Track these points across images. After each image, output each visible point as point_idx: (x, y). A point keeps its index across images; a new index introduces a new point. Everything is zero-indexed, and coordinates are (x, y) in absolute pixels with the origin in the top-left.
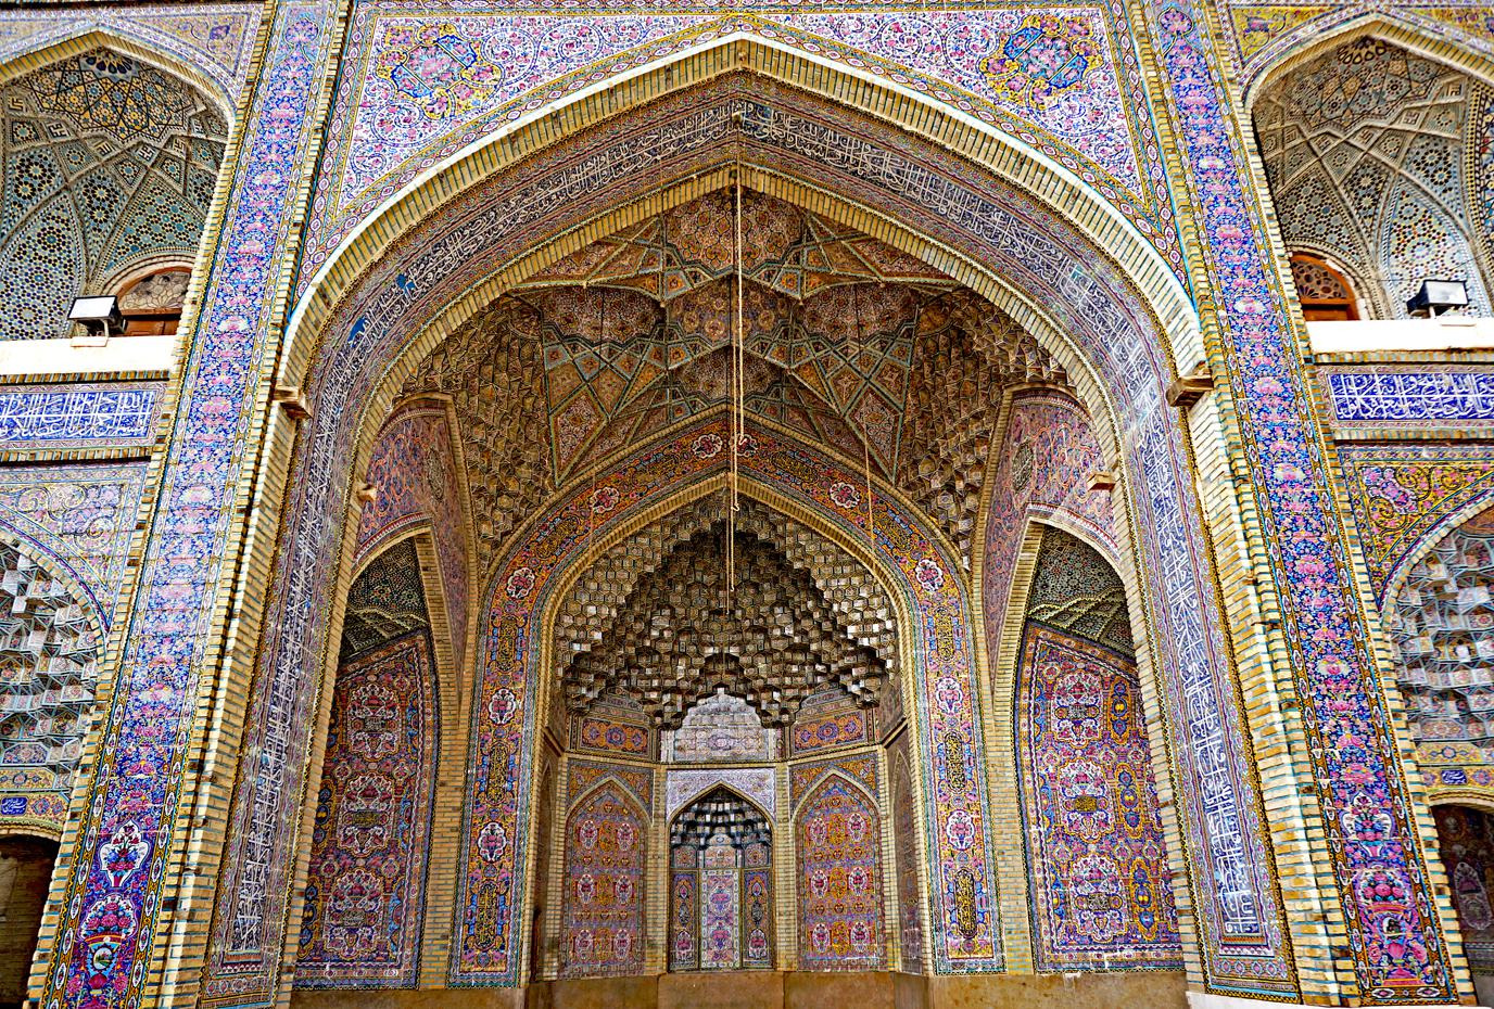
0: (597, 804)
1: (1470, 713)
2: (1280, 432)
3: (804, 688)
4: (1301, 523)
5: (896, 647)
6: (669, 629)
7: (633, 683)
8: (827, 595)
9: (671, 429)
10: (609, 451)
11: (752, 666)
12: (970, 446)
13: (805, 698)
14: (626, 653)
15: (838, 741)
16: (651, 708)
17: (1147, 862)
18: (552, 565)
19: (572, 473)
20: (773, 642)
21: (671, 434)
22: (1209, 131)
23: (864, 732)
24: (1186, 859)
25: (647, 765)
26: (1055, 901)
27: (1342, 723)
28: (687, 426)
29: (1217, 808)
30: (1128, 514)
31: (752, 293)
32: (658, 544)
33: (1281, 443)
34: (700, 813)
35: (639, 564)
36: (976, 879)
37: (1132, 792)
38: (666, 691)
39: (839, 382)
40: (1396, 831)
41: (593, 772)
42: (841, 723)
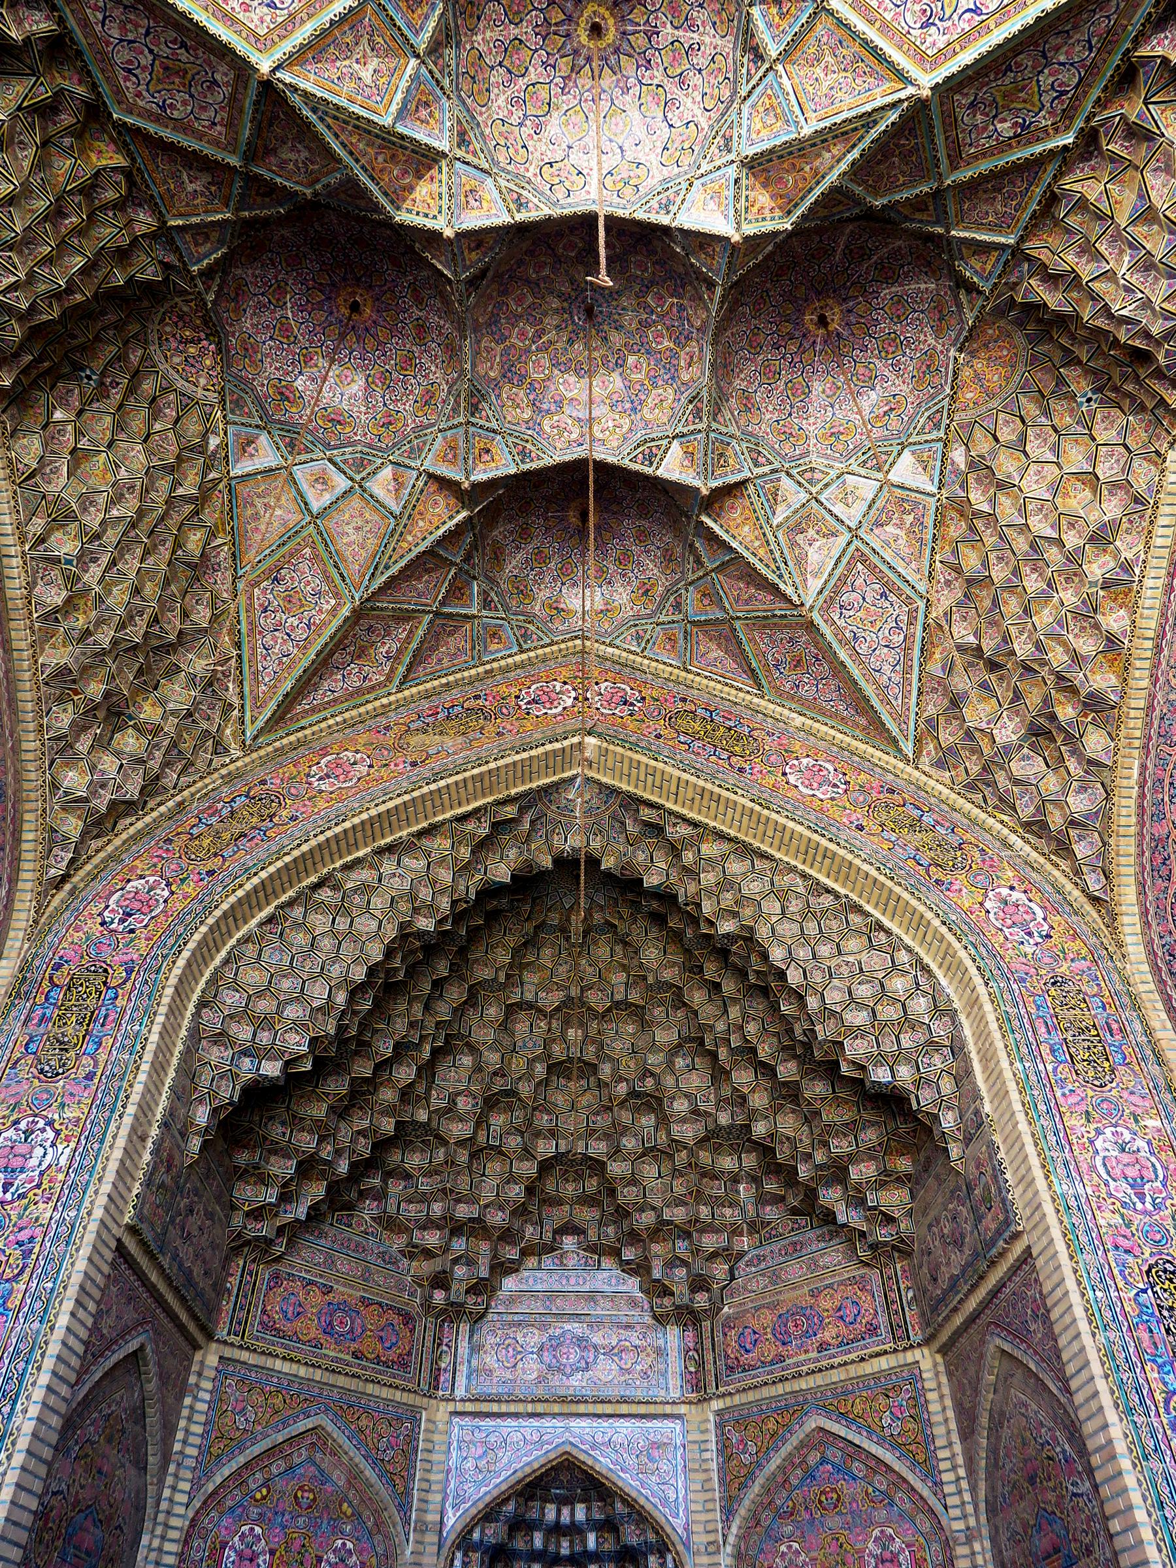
0: (279, 1484)
3: (736, 1231)
5: (963, 1076)
6: (468, 1093)
7: (392, 1209)
8: (794, 977)
9: (481, 669)
10: (359, 692)
11: (633, 1181)
12: (1087, 614)
13: (741, 1255)
14: (373, 1130)
15: (822, 1347)
16: (426, 1267)
18: (211, 873)
19: (279, 718)
20: (675, 1128)
21: (479, 678)
23: (882, 1319)
25: (406, 1398)
28: (507, 670)
31: (631, 360)
32: (445, 876)
34: (519, 1525)
35: (404, 906)
38: (457, 1229)
39: (800, 538)
41: (278, 1401)
42: (826, 1303)
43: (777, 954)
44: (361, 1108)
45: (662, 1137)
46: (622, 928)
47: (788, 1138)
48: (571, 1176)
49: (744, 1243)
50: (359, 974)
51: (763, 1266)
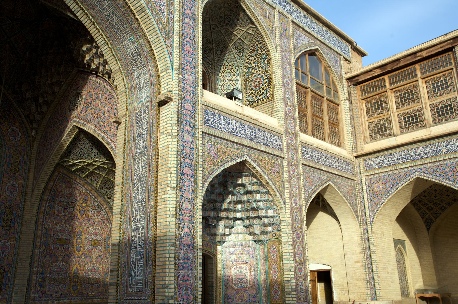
1: (209, 225)
2: (188, 124)
4: (188, 156)
17: (80, 266)
22: (190, 8)
24: (119, 265)
26: (40, 280)
27: (186, 224)
29: (136, 248)
30: (125, 136)
33: (188, 128)
36: (6, 270)
37: (81, 238)
40: (193, 259)
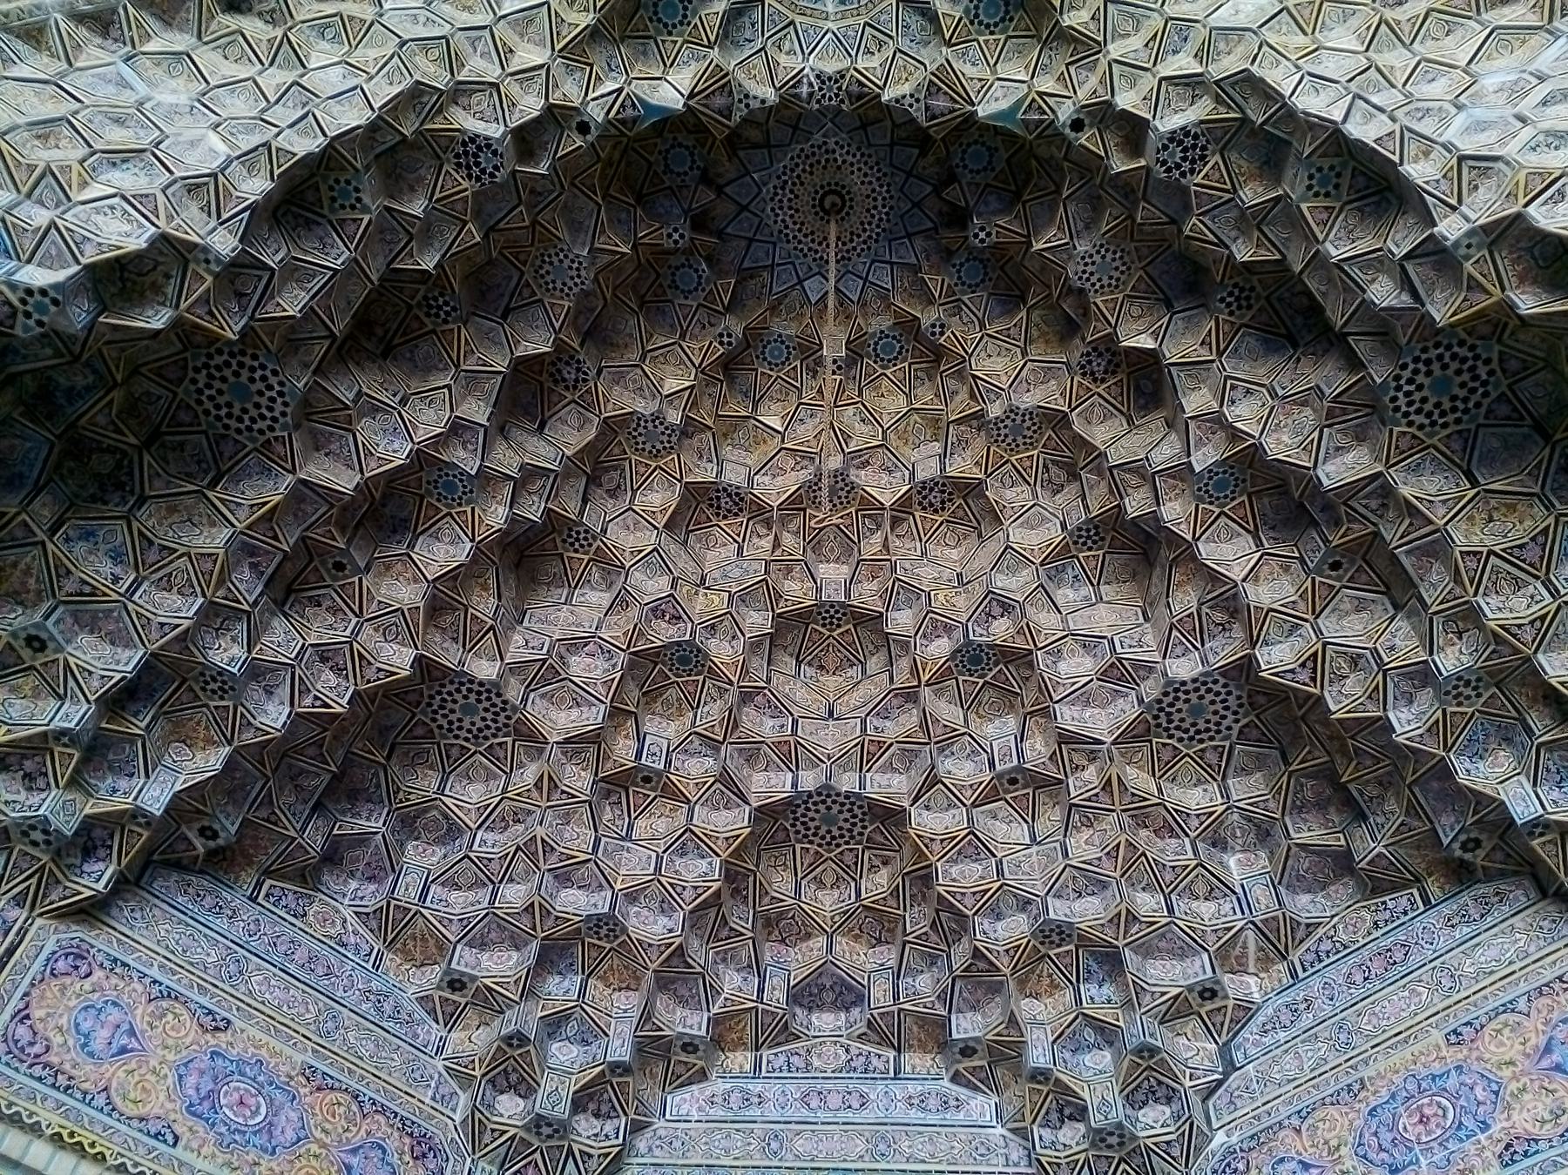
3: (1228, 955)
13: (1246, 1011)
43: (1311, 102)
44: (335, 610)
45: (1038, 749)
46: (928, 317)
47: (1354, 661)
48: (829, 871)
49: (1250, 986)
50: (305, 145)
51: (1307, 1020)
